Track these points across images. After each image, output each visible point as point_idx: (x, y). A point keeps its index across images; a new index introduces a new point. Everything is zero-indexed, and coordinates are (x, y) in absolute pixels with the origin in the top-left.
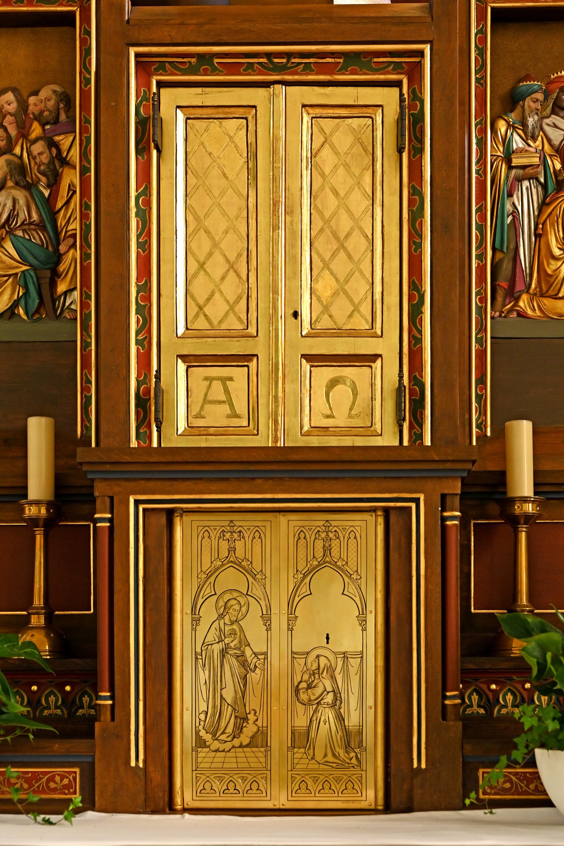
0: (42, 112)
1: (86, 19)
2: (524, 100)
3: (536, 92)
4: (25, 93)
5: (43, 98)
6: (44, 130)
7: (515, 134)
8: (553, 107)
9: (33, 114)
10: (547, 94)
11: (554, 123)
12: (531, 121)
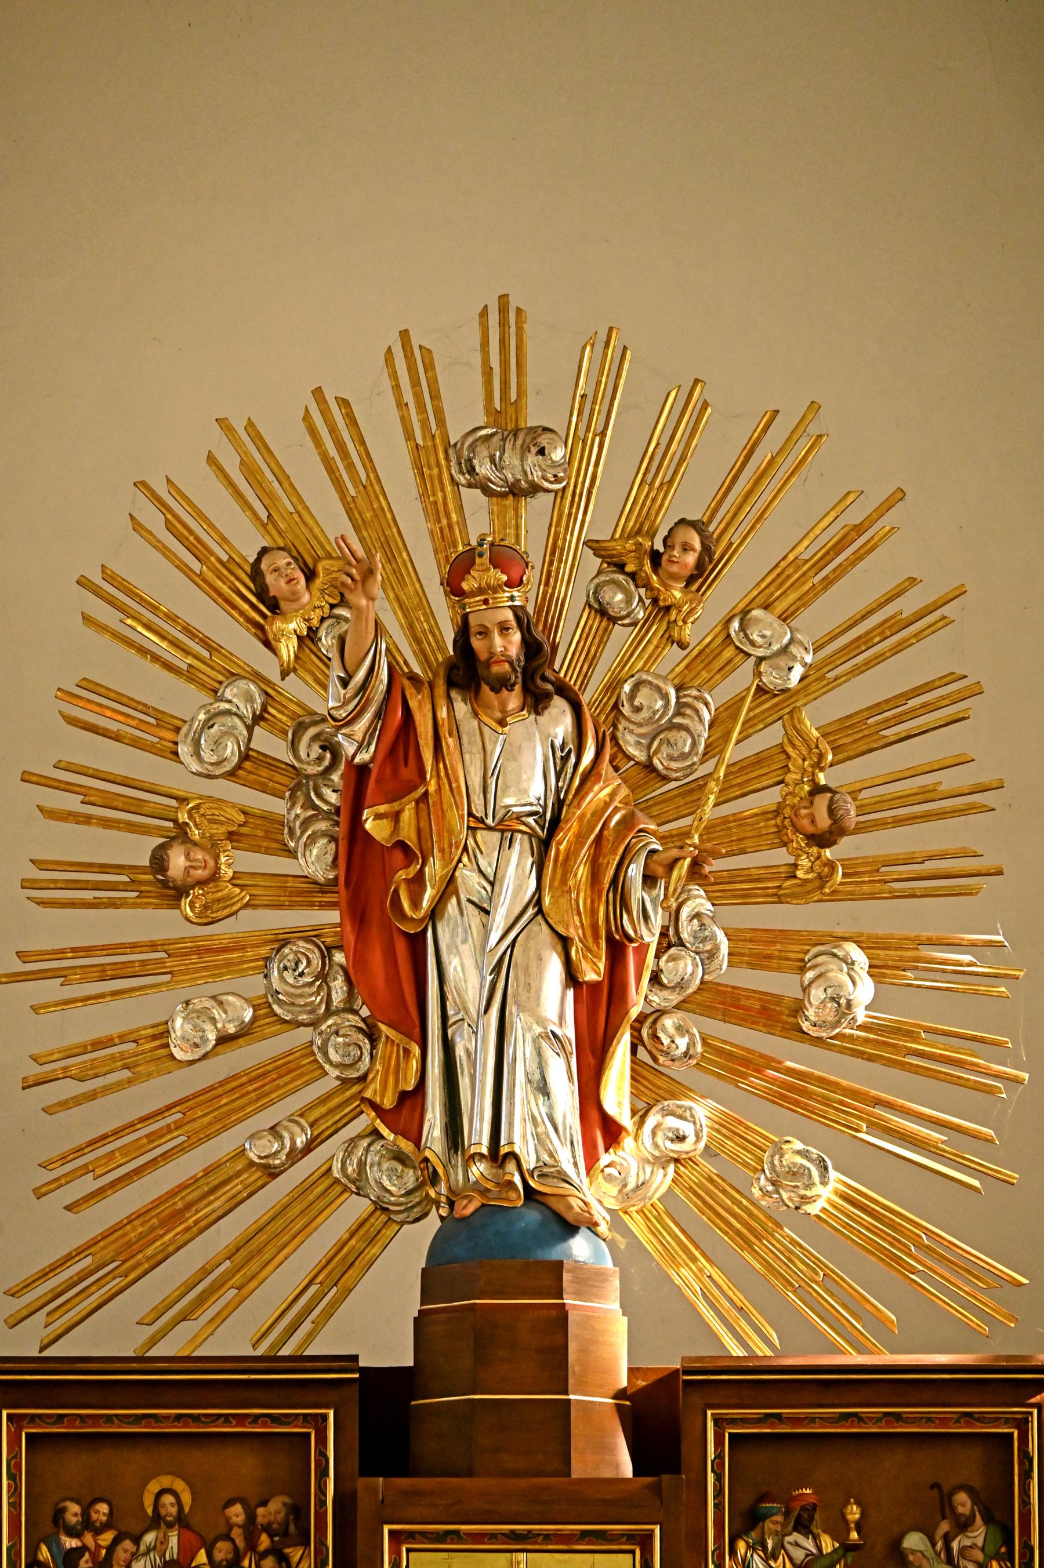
0: (270, 1524)
1: (322, 1440)
2: (764, 1522)
3: (776, 1514)
4: (253, 1502)
5: (272, 1511)
6: (272, 1541)
7: (755, 1556)
8: (795, 1524)
9: (262, 1525)
10: (787, 1514)
11: (796, 1542)
12: (770, 1544)
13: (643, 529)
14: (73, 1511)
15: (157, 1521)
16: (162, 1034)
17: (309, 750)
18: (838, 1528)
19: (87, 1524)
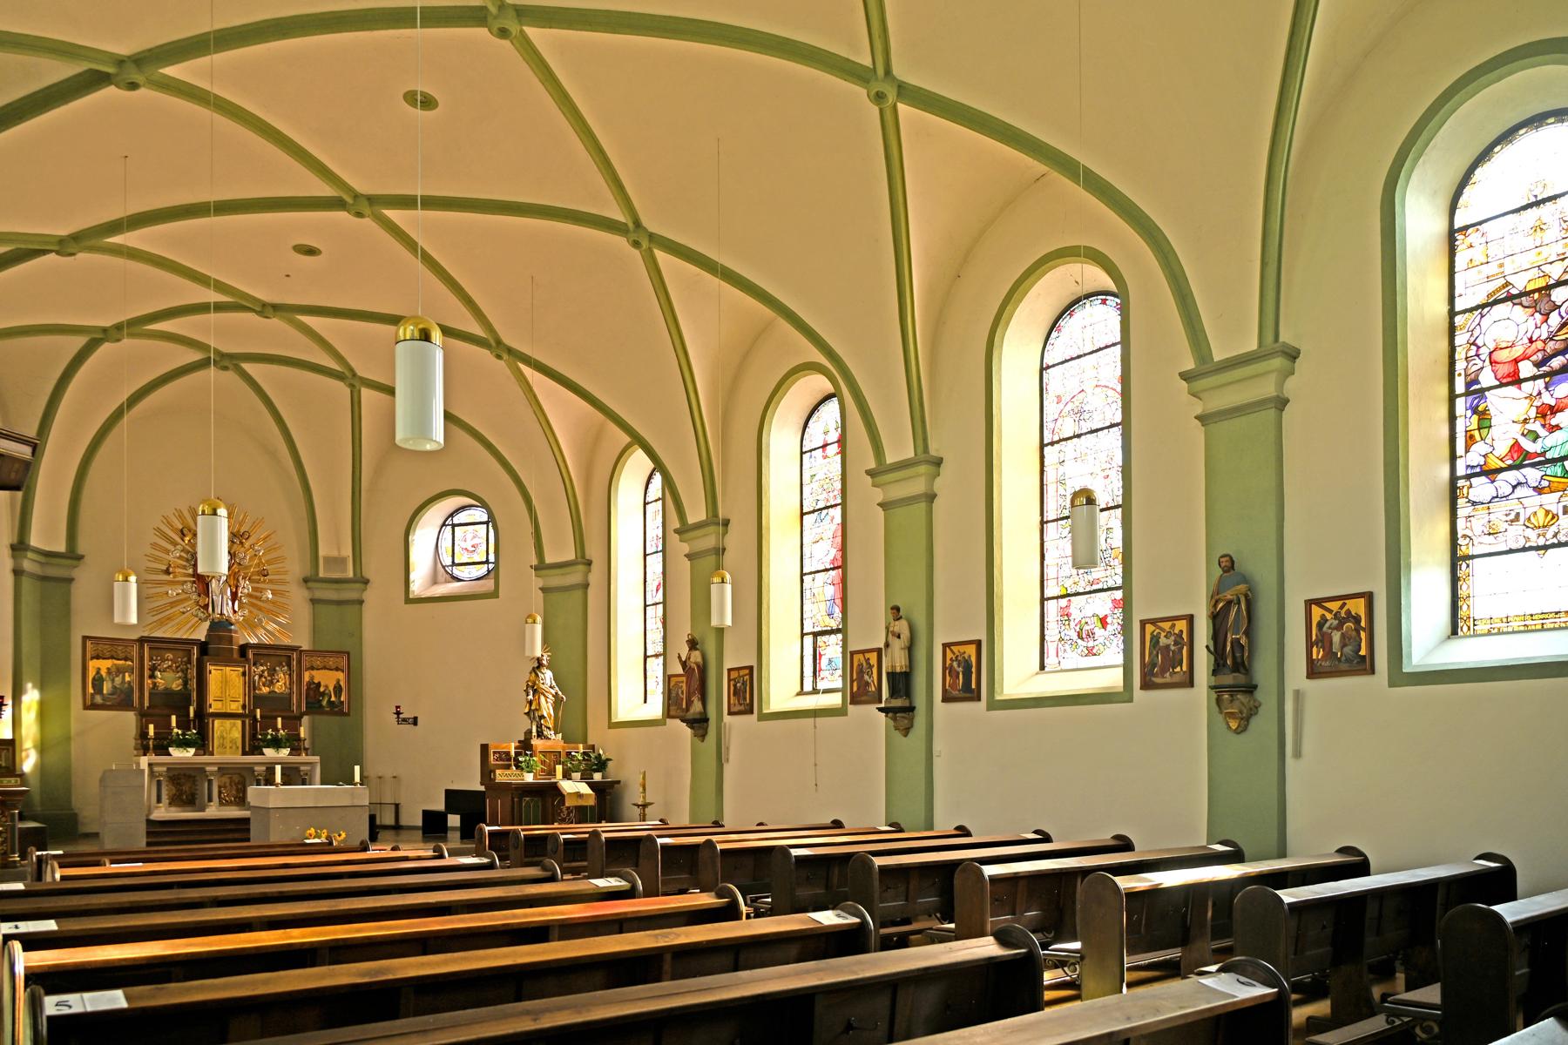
14: (154, 658)
15: (167, 660)
16: (167, 593)
18: (266, 666)
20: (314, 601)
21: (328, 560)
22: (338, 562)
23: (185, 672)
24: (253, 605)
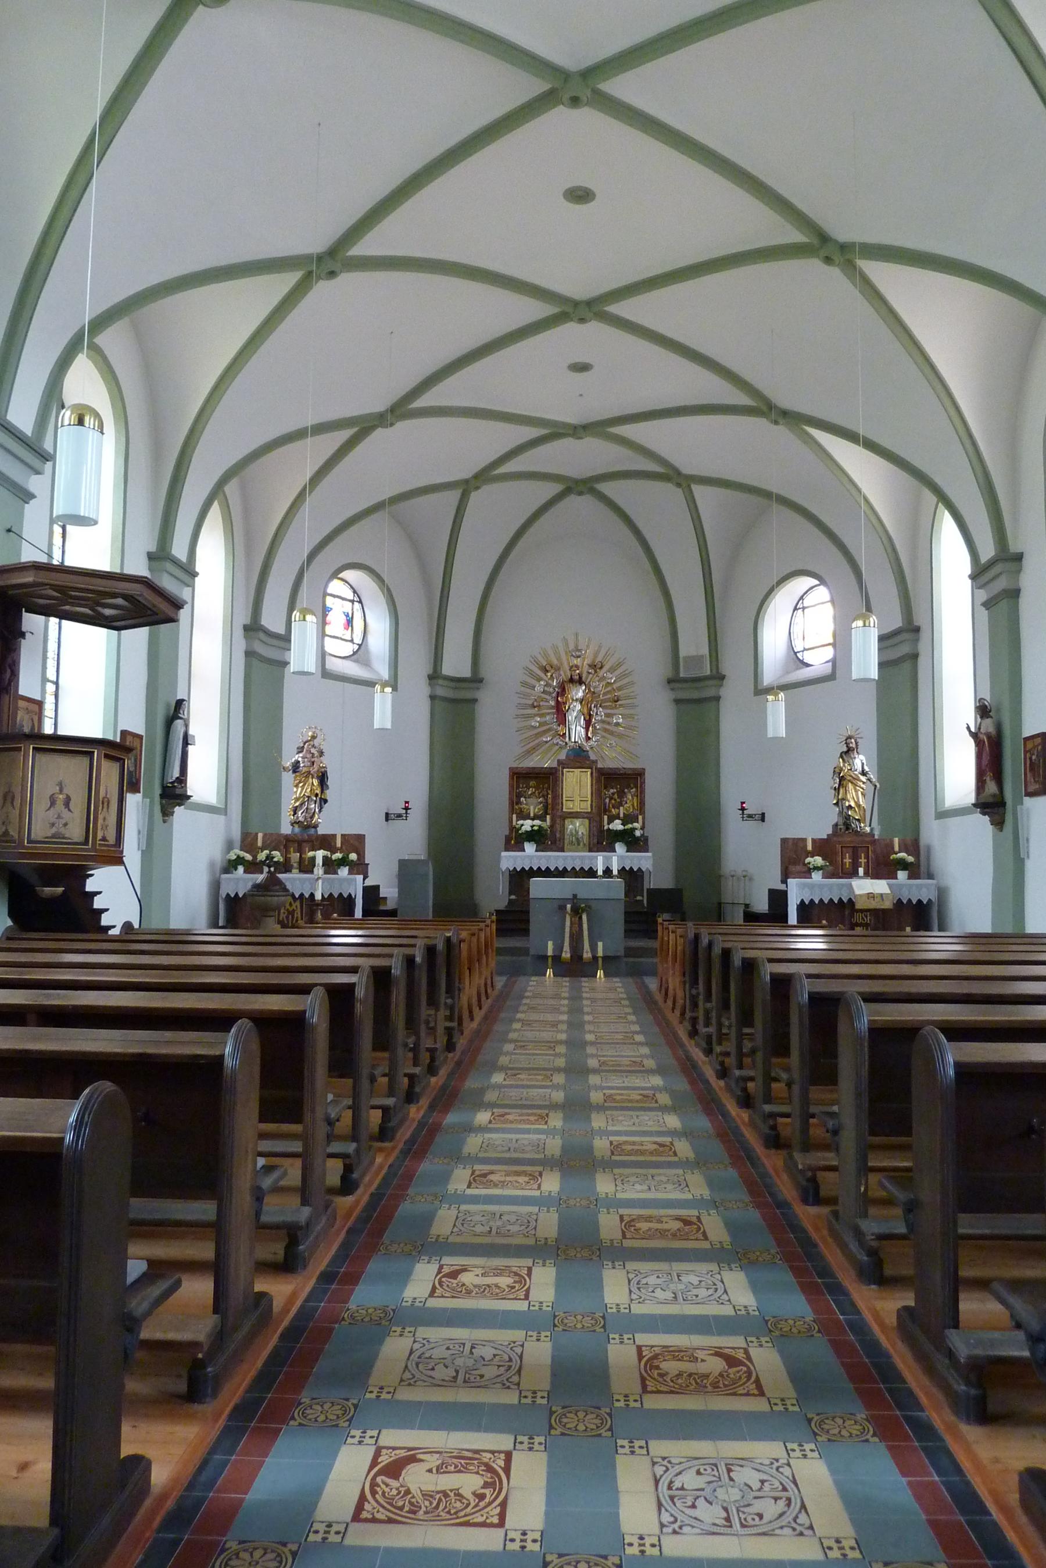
13: (594, 661)
17: (551, 690)
18: (617, 788)
19: (523, 787)
20: (677, 701)
21: (688, 659)
22: (698, 659)
23: (545, 797)
24: (606, 730)
